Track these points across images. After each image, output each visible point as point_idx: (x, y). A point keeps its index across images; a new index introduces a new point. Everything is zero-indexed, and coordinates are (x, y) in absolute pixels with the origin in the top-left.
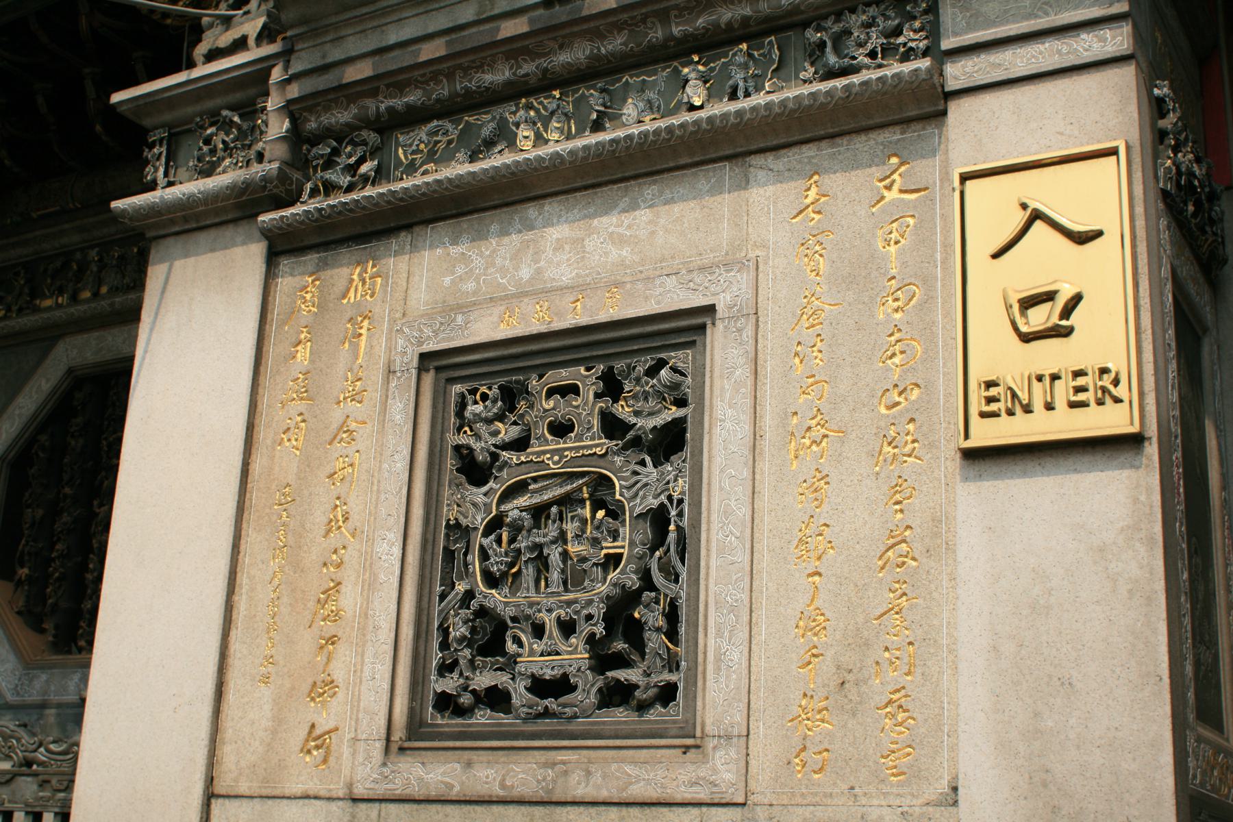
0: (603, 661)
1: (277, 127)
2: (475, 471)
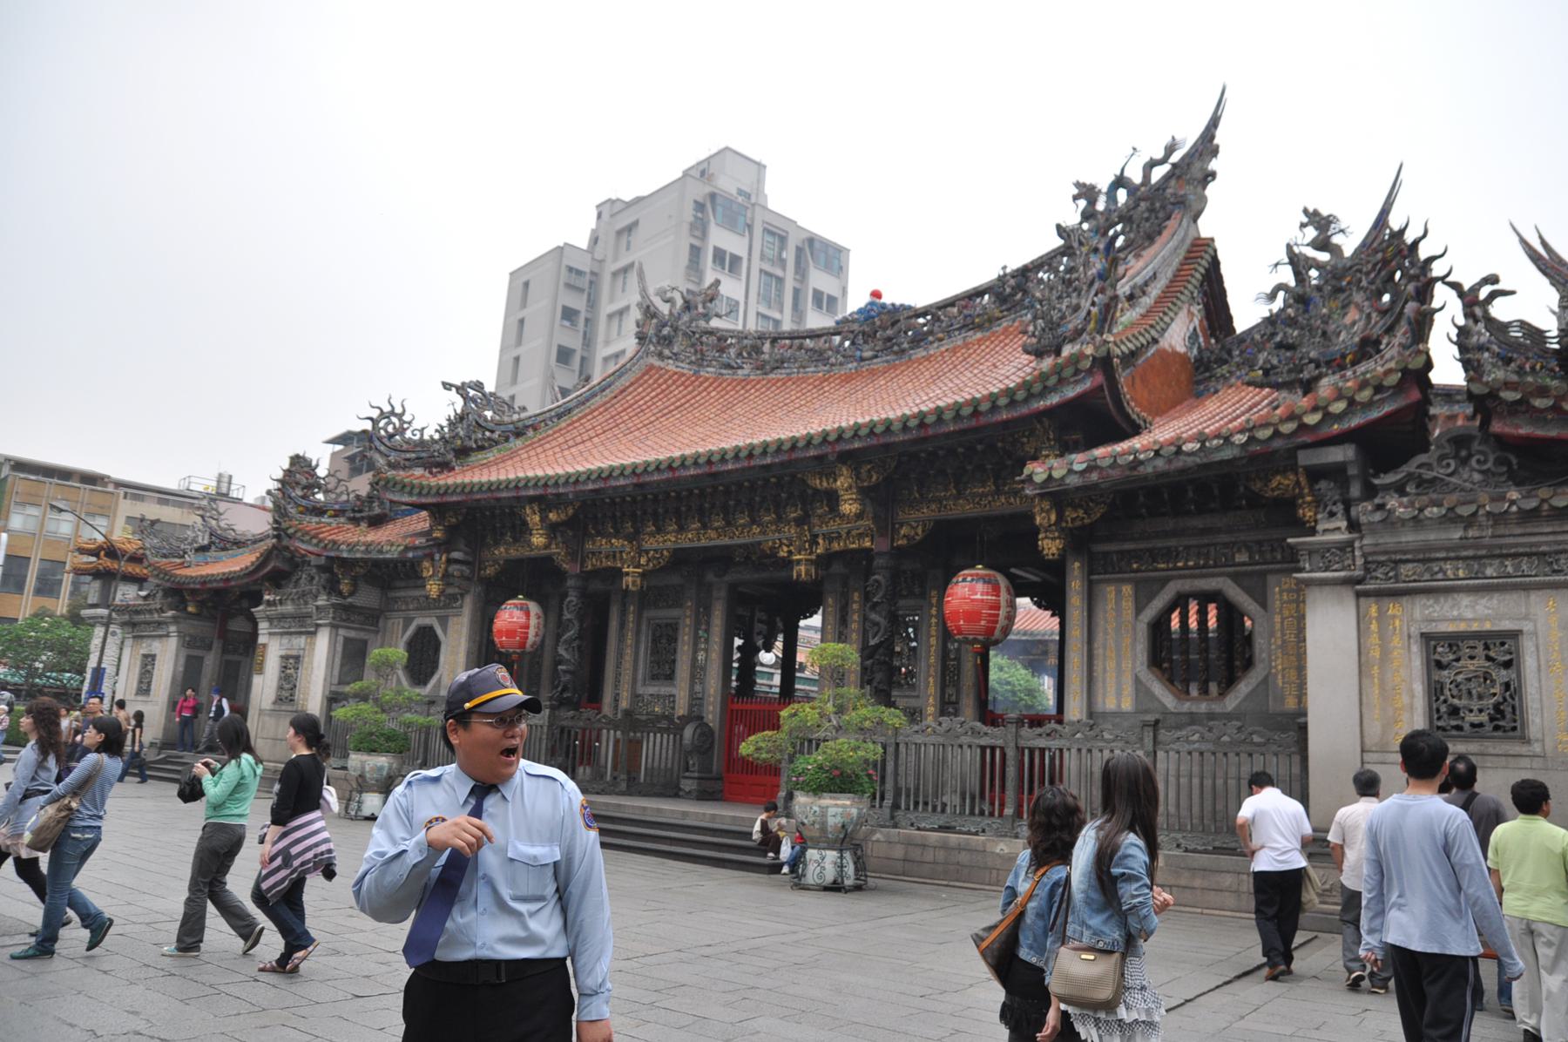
0: (1492, 719)
1: (1360, 562)
2: (1440, 665)
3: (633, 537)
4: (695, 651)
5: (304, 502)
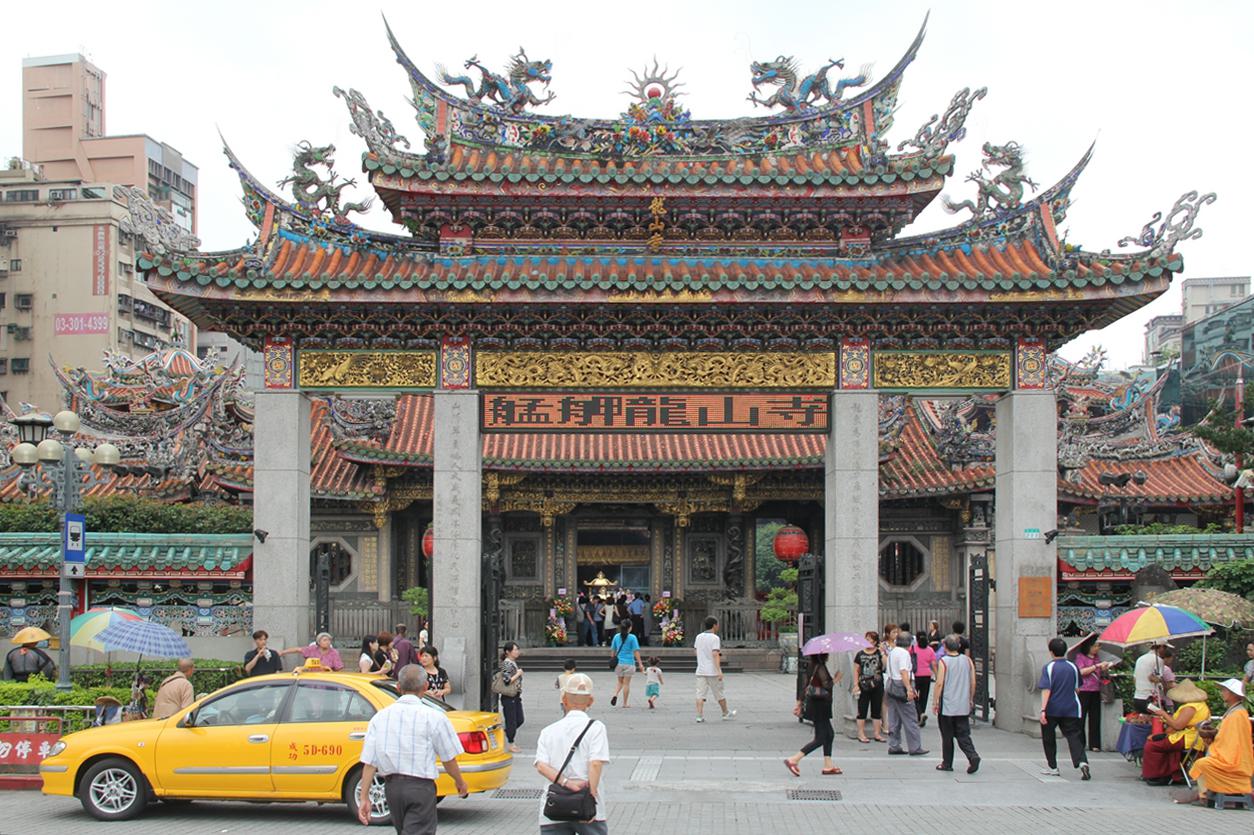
3: (549, 494)
5: (223, 450)
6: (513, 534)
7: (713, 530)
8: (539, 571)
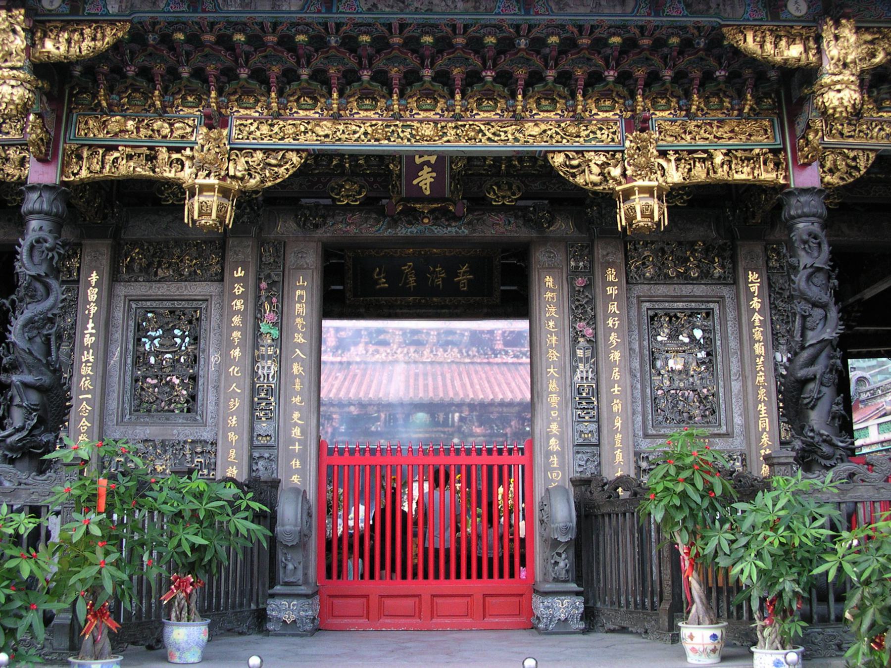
3: (215, 121)
4: (255, 361)
6: (139, 289)
7: (705, 276)
8: (208, 399)
